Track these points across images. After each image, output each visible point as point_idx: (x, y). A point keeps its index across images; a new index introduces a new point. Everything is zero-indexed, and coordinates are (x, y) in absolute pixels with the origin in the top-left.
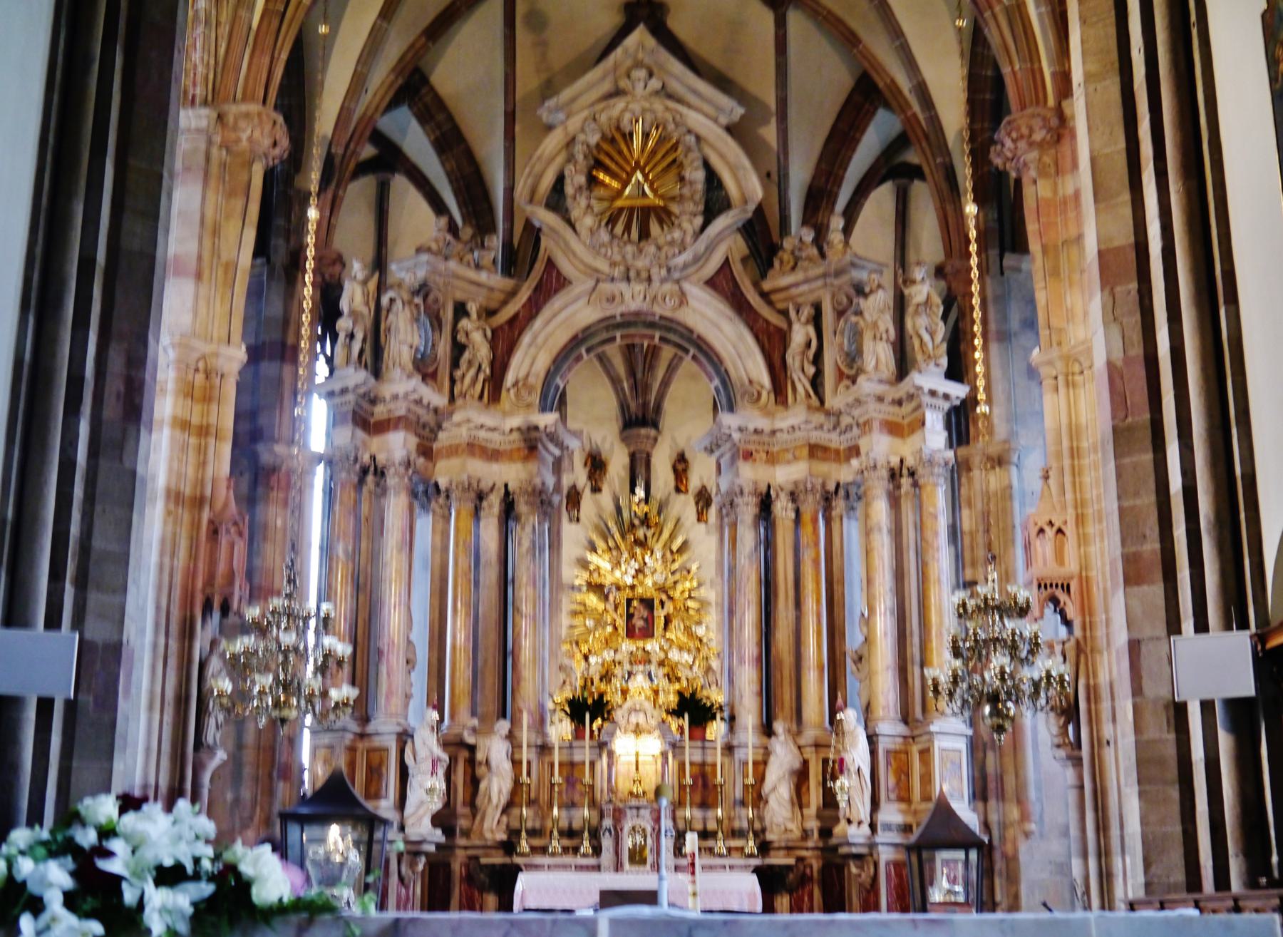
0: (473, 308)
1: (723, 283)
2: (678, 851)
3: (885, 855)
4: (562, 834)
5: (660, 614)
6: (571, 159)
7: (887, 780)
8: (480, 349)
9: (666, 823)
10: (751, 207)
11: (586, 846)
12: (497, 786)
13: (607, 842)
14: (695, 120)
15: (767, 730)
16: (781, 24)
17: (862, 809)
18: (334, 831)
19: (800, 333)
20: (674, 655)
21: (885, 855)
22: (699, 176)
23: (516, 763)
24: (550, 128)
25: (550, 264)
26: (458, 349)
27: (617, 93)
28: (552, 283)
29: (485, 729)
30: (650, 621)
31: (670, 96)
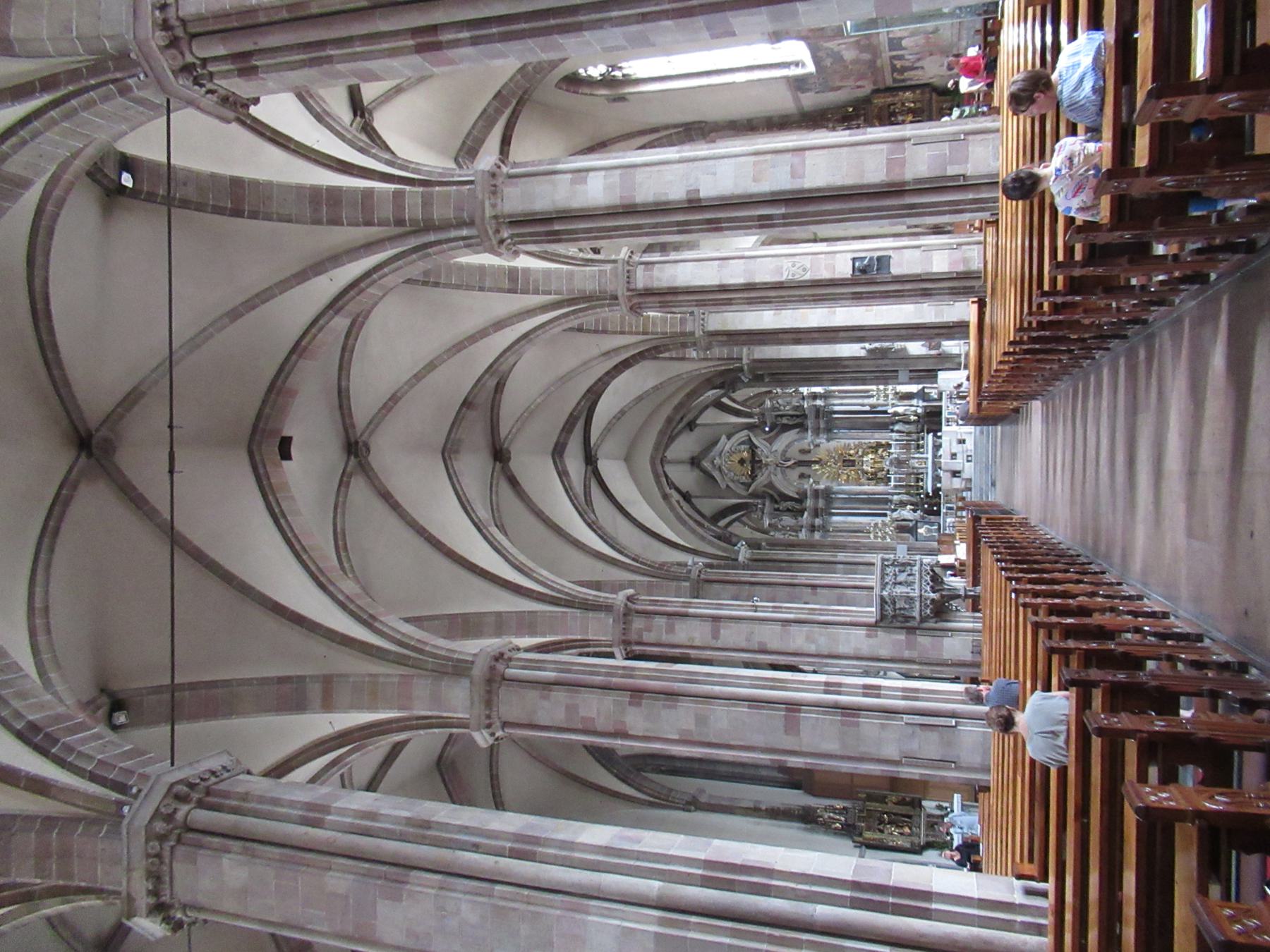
0: (776, 506)
1: (770, 441)
2: (922, 453)
3: (925, 404)
4: (918, 482)
5: (848, 458)
6: (738, 481)
7: (906, 402)
8: (789, 504)
9: (916, 456)
10: (751, 435)
11: (921, 476)
12: (905, 498)
13: (920, 471)
14: (727, 448)
15: (892, 431)
16: (699, 425)
17: (913, 409)
18: (920, 531)
19: (785, 421)
20: (860, 453)
21: (925, 404)
22: (743, 447)
23: (899, 494)
24: (727, 486)
25: (765, 486)
26: (788, 510)
27: (720, 469)
28: (770, 485)
29: (891, 501)
30: (849, 460)
31: (720, 454)
